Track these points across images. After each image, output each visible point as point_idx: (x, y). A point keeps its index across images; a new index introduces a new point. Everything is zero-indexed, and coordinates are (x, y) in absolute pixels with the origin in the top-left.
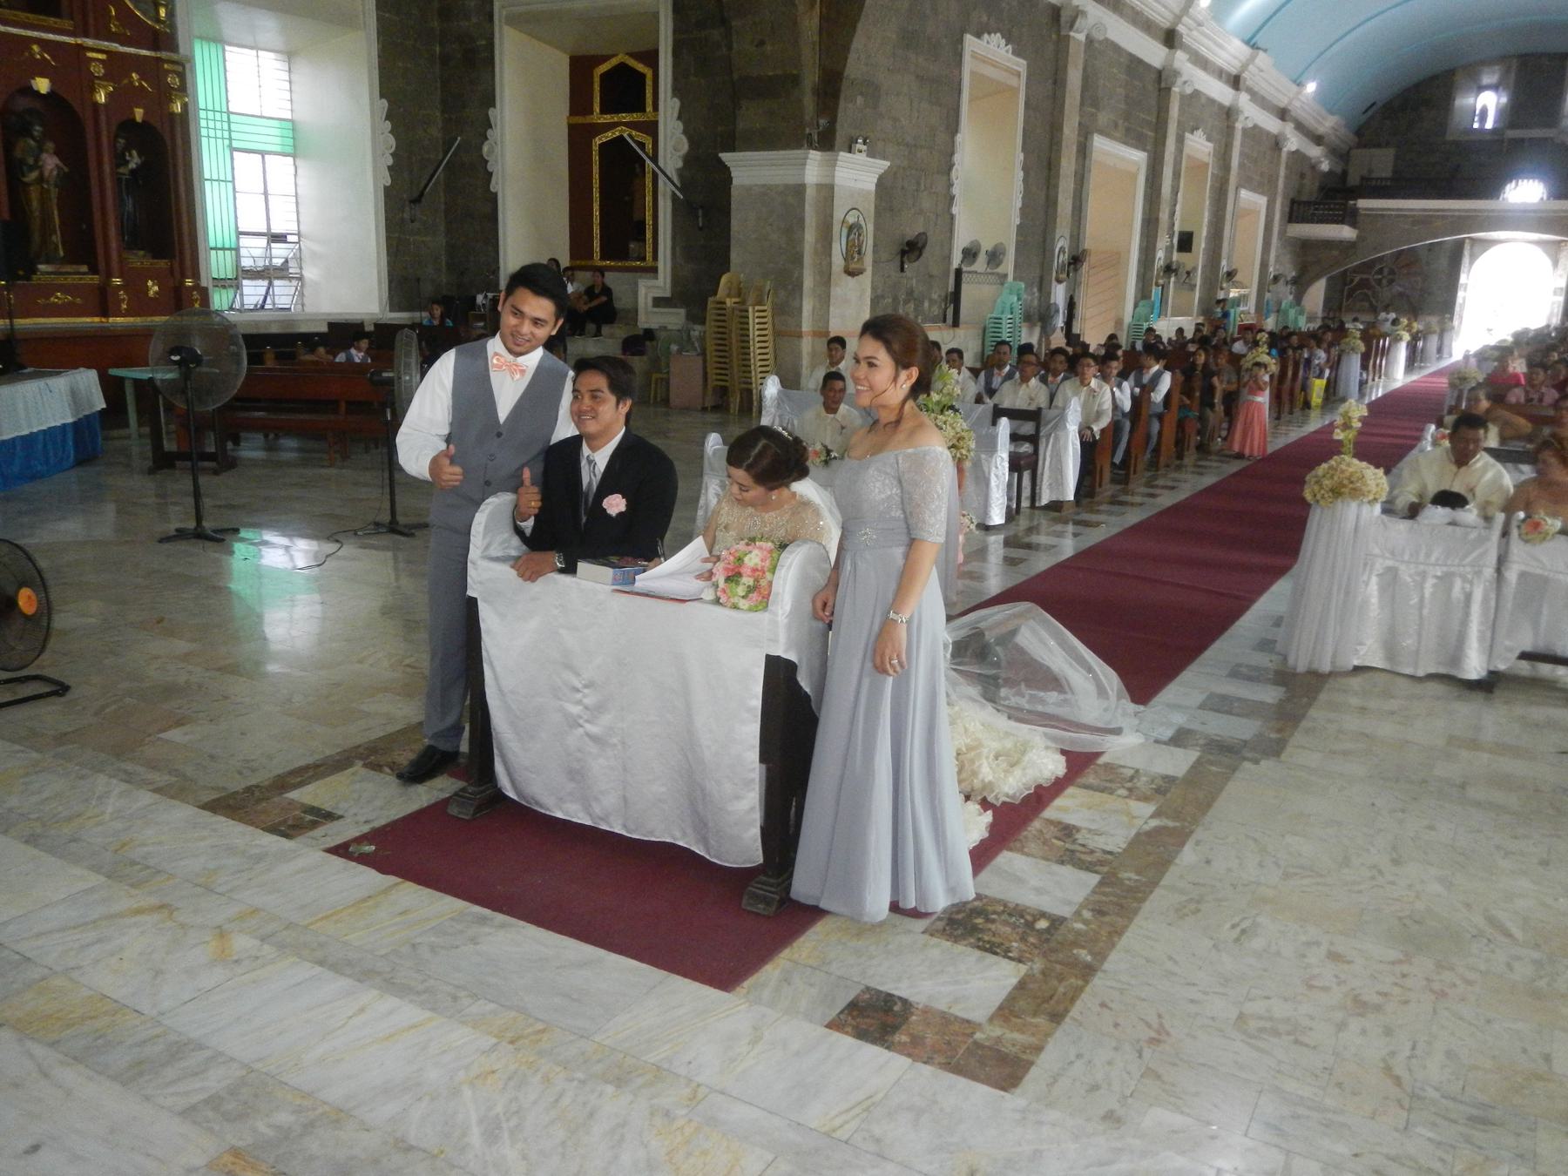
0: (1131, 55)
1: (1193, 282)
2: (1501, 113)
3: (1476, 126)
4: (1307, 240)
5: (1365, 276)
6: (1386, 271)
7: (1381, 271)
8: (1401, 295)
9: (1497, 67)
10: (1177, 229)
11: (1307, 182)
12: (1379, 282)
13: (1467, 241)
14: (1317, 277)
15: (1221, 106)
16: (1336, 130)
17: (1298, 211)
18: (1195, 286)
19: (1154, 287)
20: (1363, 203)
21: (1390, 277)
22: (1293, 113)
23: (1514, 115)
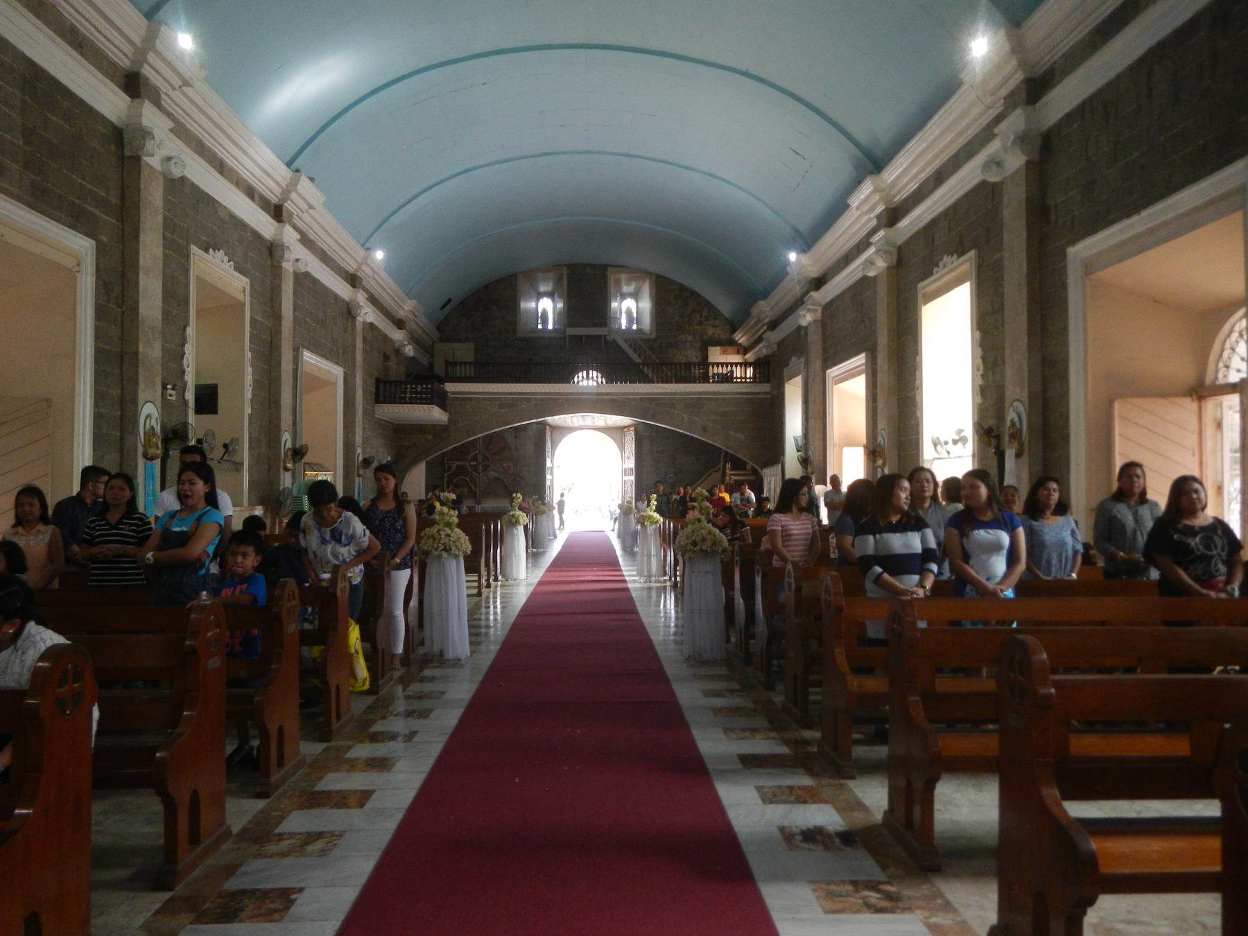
0: (31, 64)
1: (236, 459)
2: (558, 317)
3: (540, 327)
6: (480, 457)
7: (475, 458)
8: (496, 479)
9: (550, 274)
10: (190, 378)
11: (392, 364)
12: (475, 468)
13: (548, 428)
15: (257, 236)
16: (414, 314)
17: (384, 390)
18: (242, 464)
19: (141, 462)
20: (450, 387)
21: (486, 463)
22: (365, 283)
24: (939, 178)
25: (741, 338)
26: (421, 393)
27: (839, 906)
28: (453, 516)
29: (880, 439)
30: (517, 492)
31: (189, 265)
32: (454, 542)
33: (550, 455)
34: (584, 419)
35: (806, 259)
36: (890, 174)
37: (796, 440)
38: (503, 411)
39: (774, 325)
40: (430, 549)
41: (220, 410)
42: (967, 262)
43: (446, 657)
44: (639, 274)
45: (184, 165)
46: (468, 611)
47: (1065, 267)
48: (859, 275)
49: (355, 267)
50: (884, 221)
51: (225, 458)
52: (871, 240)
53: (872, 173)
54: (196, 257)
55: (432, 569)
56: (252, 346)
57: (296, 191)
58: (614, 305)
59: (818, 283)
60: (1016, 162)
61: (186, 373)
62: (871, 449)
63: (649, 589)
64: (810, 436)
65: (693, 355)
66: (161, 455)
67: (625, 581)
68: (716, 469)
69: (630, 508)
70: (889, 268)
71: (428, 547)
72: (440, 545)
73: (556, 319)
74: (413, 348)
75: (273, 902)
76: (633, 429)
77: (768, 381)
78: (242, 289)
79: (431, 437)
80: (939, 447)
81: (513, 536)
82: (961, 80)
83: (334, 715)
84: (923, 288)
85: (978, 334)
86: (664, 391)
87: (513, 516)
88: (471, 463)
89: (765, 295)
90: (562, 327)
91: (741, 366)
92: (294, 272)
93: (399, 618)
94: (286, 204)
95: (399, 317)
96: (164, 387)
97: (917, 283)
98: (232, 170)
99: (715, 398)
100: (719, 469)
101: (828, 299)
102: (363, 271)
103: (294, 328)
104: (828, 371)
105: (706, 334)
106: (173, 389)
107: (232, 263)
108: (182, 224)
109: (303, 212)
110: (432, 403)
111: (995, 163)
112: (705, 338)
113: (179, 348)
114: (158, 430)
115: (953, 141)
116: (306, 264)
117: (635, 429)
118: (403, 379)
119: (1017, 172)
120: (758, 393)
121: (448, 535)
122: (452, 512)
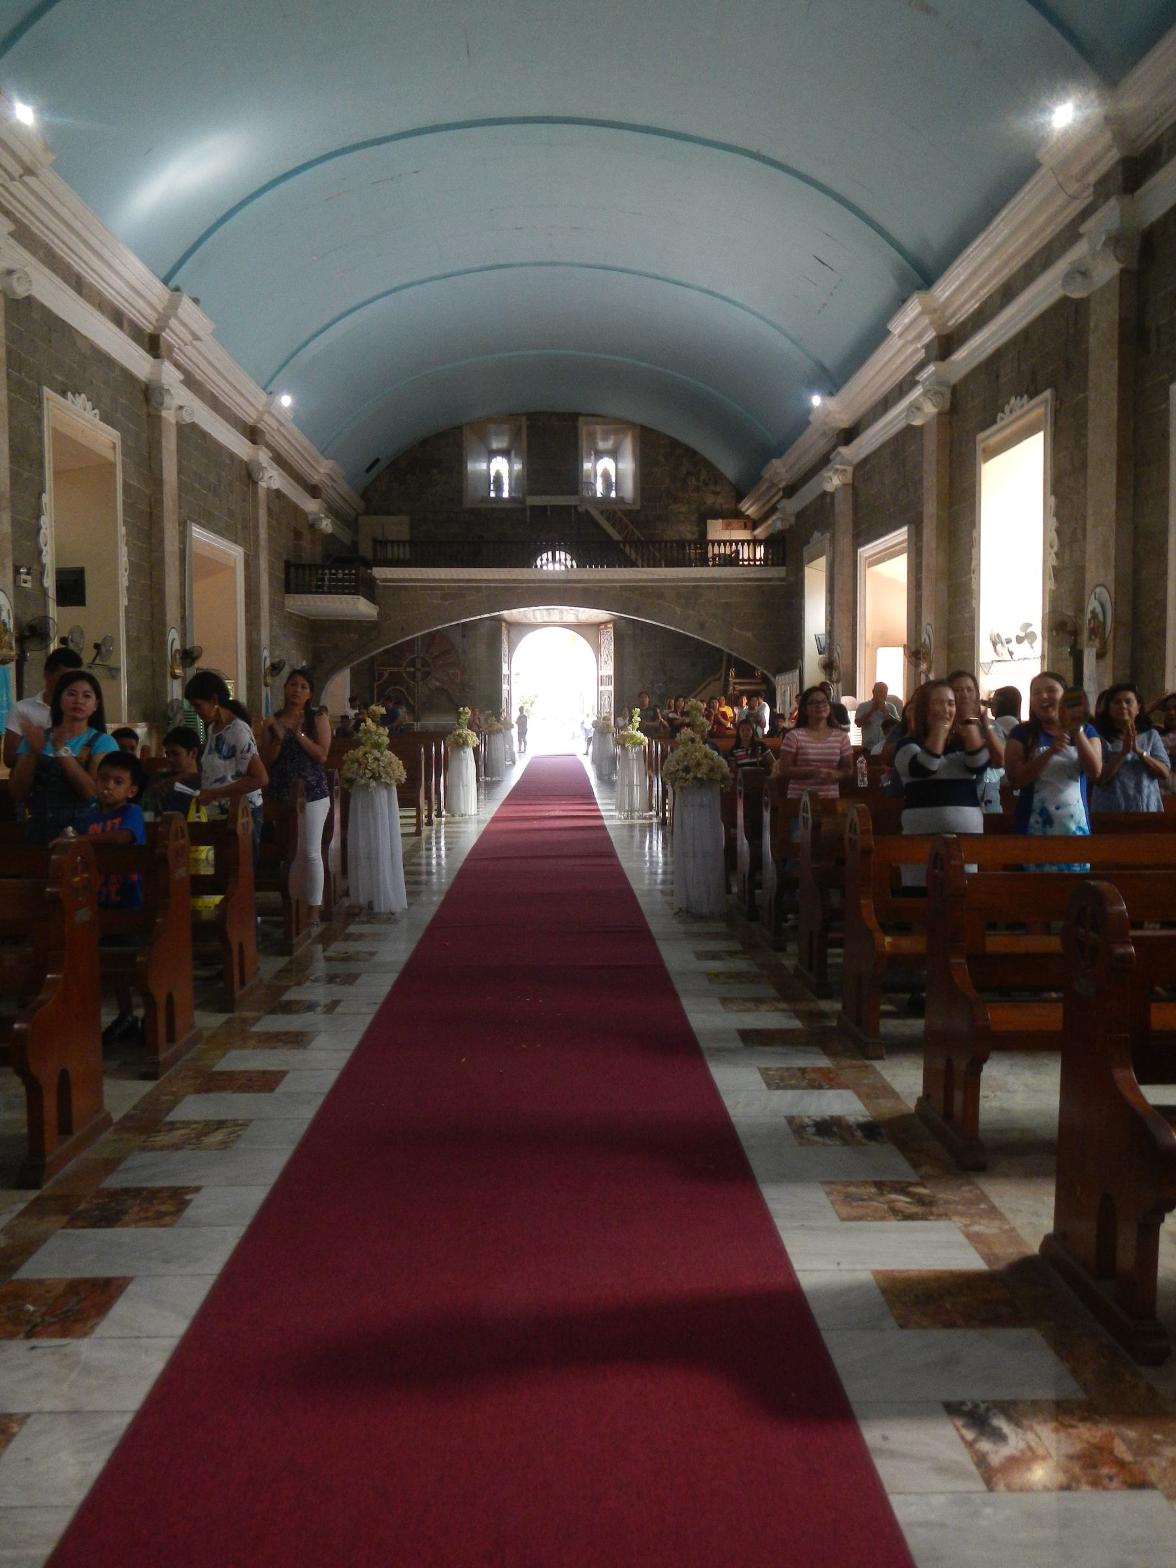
1: (111, 662)
2: (515, 482)
3: (492, 495)
4: (314, 621)
5: (396, 669)
7: (412, 663)
9: (505, 427)
11: (306, 542)
12: (413, 676)
13: (504, 624)
14: (336, 668)
15: (128, 376)
16: (331, 478)
18: (118, 670)
20: (379, 573)
21: (427, 669)
22: (268, 437)
23: (531, 481)
24: (1007, 293)
25: (750, 509)
26: (340, 580)
27: (860, 1212)
28: (383, 735)
29: (924, 637)
30: (464, 706)
31: (42, 411)
32: (384, 767)
33: (506, 659)
34: (549, 613)
35: (833, 404)
36: (944, 290)
37: (818, 639)
38: (447, 603)
39: (790, 491)
40: (354, 776)
41: (87, 603)
42: (1040, 406)
43: (376, 909)
44: (618, 425)
45: (30, 281)
46: (404, 854)
47: (1167, 410)
48: (901, 425)
49: (255, 418)
50: (935, 352)
51: (97, 662)
52: (918, 378)
53: (919, 288)
54: (51, 403)
55: (357, 803)
56: (128, 519)
57: (176, 316)
58: (587, 466)
59: (849, 435)
60: (1107, 270)
61: (44, 553)
62: (913, 649)
63: (631, 826)
64: (836, 633)
65: (687, 531)
66: (16, 658)
67: (600, 817)
68: (717, 676)
69: (608, 726)
70: (940, 414)
71: (353, 773)
72: (367, 771)
73: (513, 483)
74: (332, 522)
75: (163, 1203)
76: (611, 625)
77: (783, 564)
78: (111, 445)
79: (355, 636)
80: (999, 647)
81: (460, 760)
82: (1038, 160)
83: (237, 978)
84: (982, 441)
85: (1052, 500)
86: (650, 577)
87: (460, 735)
88: (408, 670)
89: (780, 453)
90: (521, 495)
91: (749, 545)
92: (177, 423)
93: (317, 861)
94: (163, 334)
95: (313, 482)
96: (17, 571)
97: (976, 434)
98: (92, 287)
99: (714, 586)
100: (721, 676)
101: (862, 456)
102: (265, 422)
103: (180, 497)
104: (860, 550)
105: (705, 503)
106: (28, 573)
107: (96, 411)
108: (31, 360)
109: (186, 344)
110: (356, 593)
111: (1081, 272)
112: (703, 508)
113: (34, 521)
114: (11, 625)
115: (1025, 244)
116: (192, 413)
117: (614, 626)
118: (319, 562)
119: (1108, 285)
120: (769, 580)
121: (377, 759)
122: (381, 730)
